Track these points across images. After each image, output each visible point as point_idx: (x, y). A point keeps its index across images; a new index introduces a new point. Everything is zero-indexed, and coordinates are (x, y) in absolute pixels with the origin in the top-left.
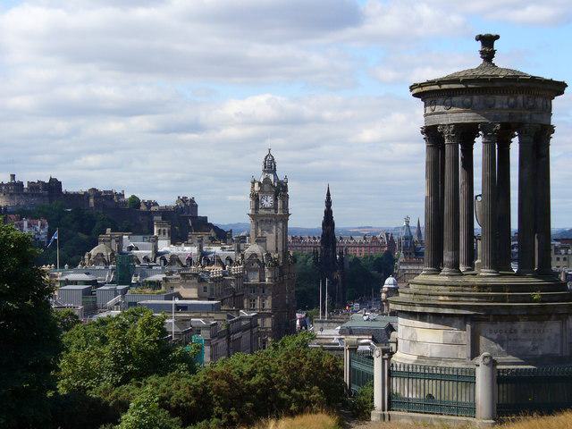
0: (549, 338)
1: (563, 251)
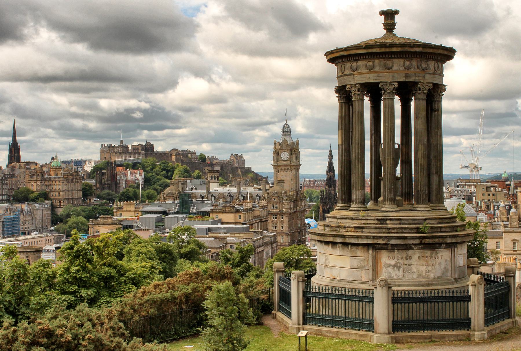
1: (492, 189)
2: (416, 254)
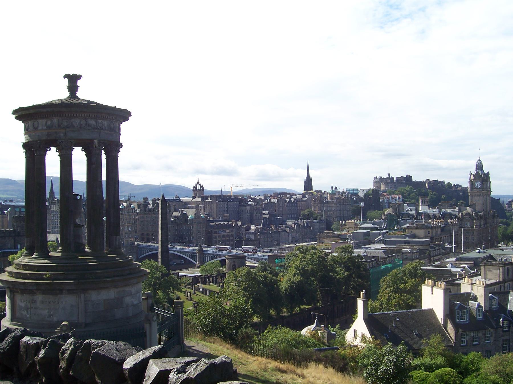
2: (39, 297)
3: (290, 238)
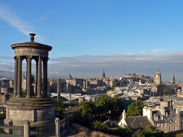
0: (27, 116)
3: (98, 92)
